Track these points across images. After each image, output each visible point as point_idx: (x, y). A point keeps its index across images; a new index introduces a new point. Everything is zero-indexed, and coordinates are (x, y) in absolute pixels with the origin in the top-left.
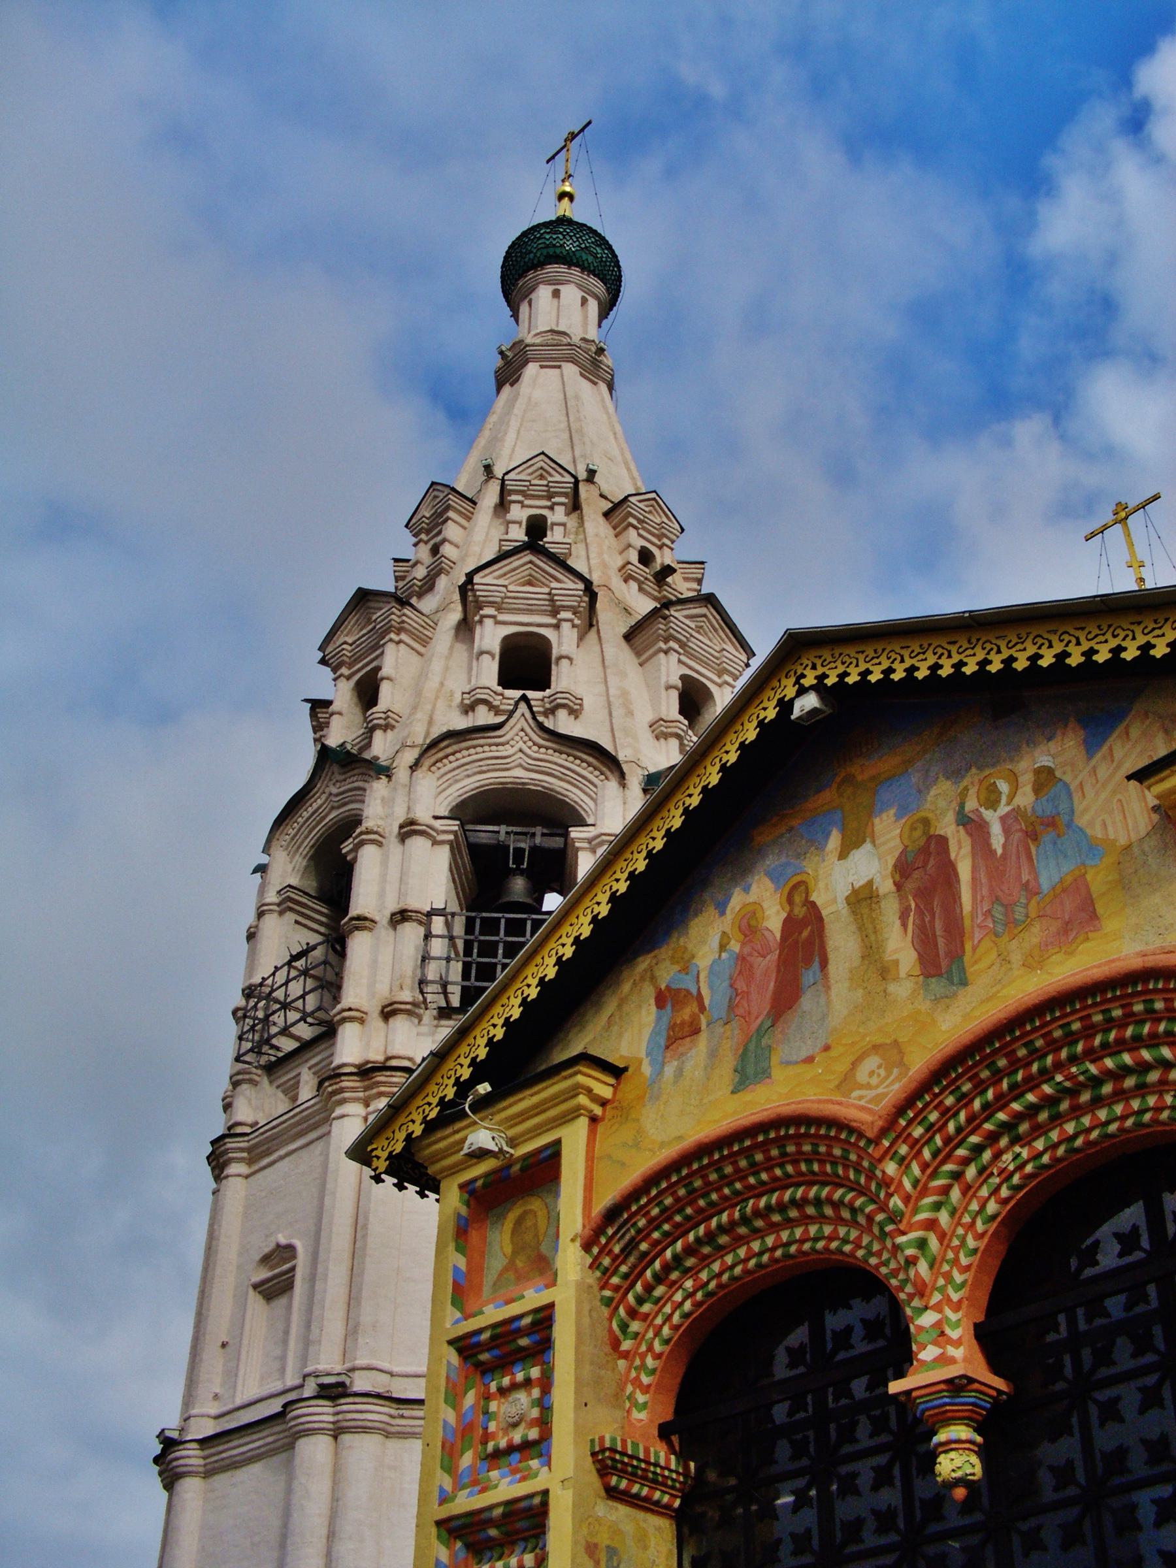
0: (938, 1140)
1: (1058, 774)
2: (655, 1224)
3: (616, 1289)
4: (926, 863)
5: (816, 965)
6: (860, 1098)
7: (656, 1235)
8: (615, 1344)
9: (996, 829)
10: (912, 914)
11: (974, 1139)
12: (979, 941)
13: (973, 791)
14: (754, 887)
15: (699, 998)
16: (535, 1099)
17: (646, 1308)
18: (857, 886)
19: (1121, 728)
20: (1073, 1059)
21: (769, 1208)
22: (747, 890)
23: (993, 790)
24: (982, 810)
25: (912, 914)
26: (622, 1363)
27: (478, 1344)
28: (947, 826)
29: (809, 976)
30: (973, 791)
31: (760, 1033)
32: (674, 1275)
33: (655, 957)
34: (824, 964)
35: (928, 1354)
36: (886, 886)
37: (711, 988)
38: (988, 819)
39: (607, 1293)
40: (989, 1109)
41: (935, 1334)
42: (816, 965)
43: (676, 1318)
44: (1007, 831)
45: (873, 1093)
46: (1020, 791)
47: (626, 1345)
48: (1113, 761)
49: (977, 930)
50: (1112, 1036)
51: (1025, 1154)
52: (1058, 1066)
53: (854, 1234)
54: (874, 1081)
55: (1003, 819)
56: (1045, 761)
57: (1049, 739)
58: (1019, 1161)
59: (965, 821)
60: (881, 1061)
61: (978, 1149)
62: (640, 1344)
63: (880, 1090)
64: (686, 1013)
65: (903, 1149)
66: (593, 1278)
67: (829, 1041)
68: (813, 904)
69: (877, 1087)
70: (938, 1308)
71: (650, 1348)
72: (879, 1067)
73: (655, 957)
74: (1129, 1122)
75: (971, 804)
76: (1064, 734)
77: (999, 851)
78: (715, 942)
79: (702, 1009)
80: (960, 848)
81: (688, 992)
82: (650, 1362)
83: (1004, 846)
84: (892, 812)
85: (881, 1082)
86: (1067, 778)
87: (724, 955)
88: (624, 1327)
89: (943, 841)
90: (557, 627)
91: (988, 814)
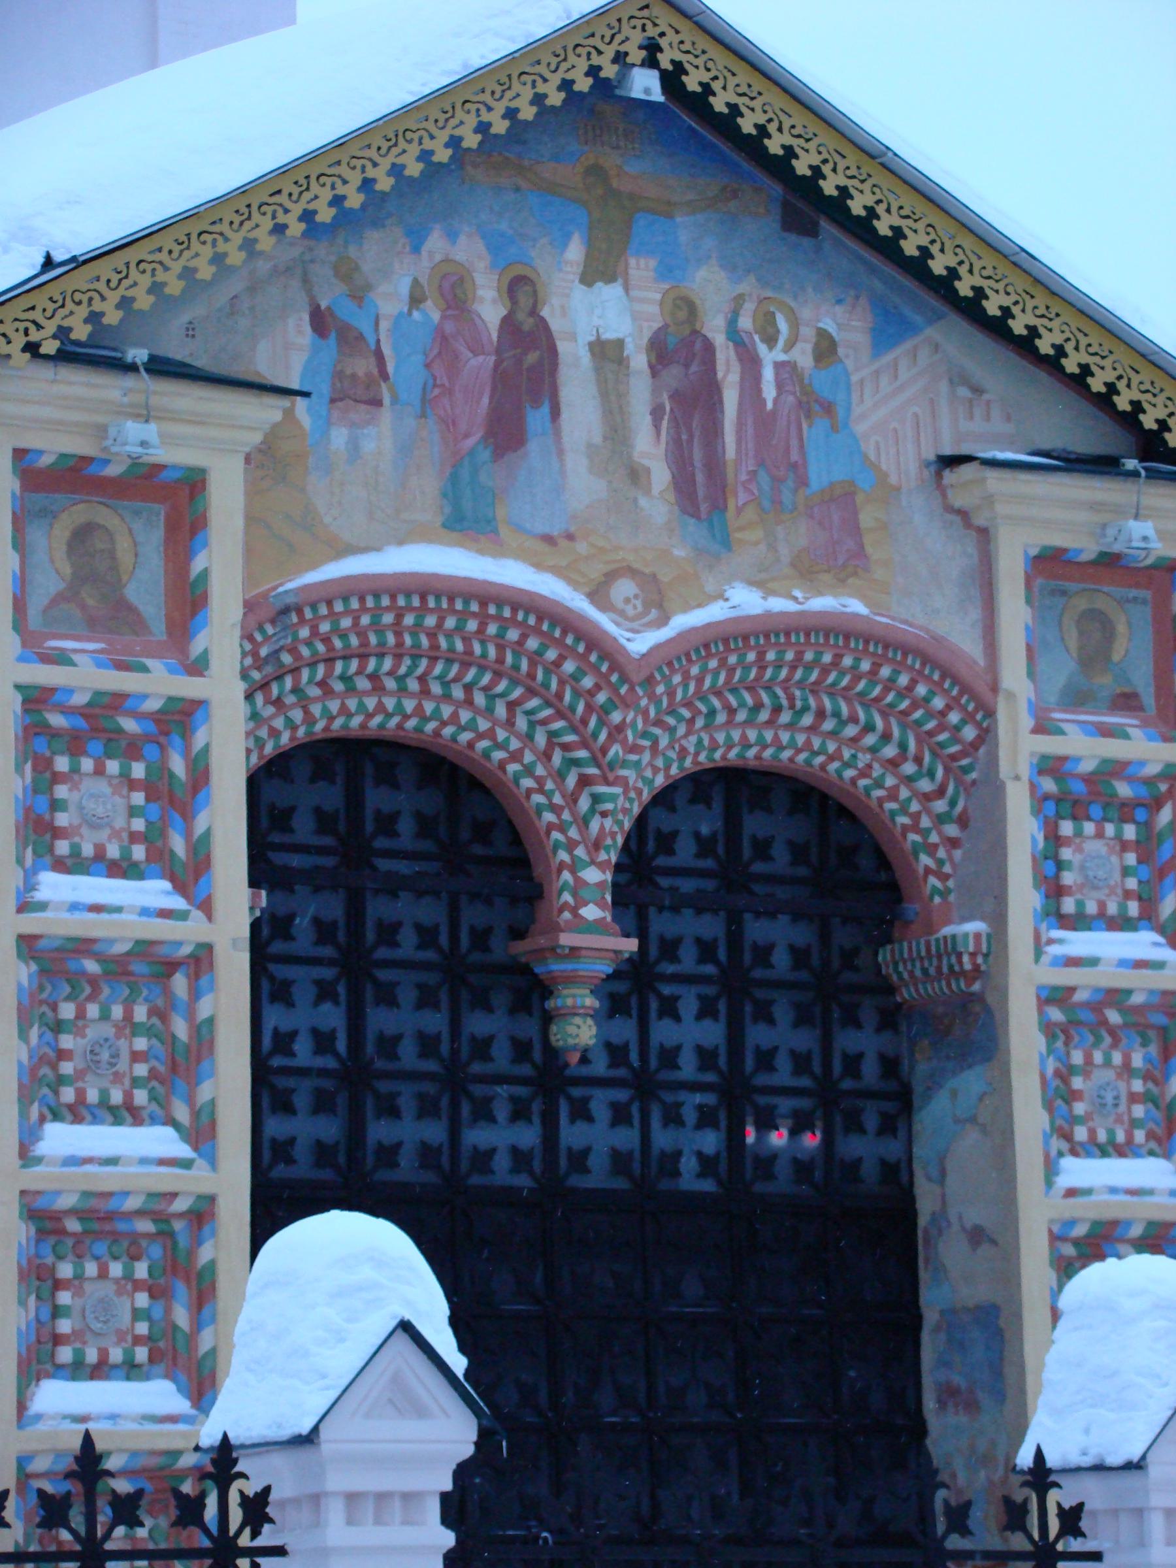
1: (841, 351)
4: (687, 366)
9: (768, 374)
10: (666, 417)
12: (744, 504)
13: (749, 307)
14: (463, 239)
19: (908, 345)
22: (452, 236)
23: (770, 318)
24: (756, 338)
25: (666, 417)
28: (715, 328)
29: (537, 419)
30: (749, 307)
33: (311, 249)
34: (555, 413)
36: (639, 361)
38: (762, 356)
41: (598, 896)
42: (546, 409)
44: (780, 386)
46: (799, 346)
48: (896, 377)
49: (740, 490)
53: (515, 744)
55: (778, 366)
56: (829, 325)
57: (839, 302)
64: (362, 366)
67: (573, 529)
68: (543, 320)
72: (636, 597)
73: (311, 249)
75: (745, 322)
76: (854, 306)
77: (770, 405)
78: (404, 287)
79: (384, 376)
80: (728, 371)
81: (361, 337)
83: (776, 401)
84: (653, 263)
86: (850, 364)
87: (416, 314)
89: (709, 348)
91: (762, 348)
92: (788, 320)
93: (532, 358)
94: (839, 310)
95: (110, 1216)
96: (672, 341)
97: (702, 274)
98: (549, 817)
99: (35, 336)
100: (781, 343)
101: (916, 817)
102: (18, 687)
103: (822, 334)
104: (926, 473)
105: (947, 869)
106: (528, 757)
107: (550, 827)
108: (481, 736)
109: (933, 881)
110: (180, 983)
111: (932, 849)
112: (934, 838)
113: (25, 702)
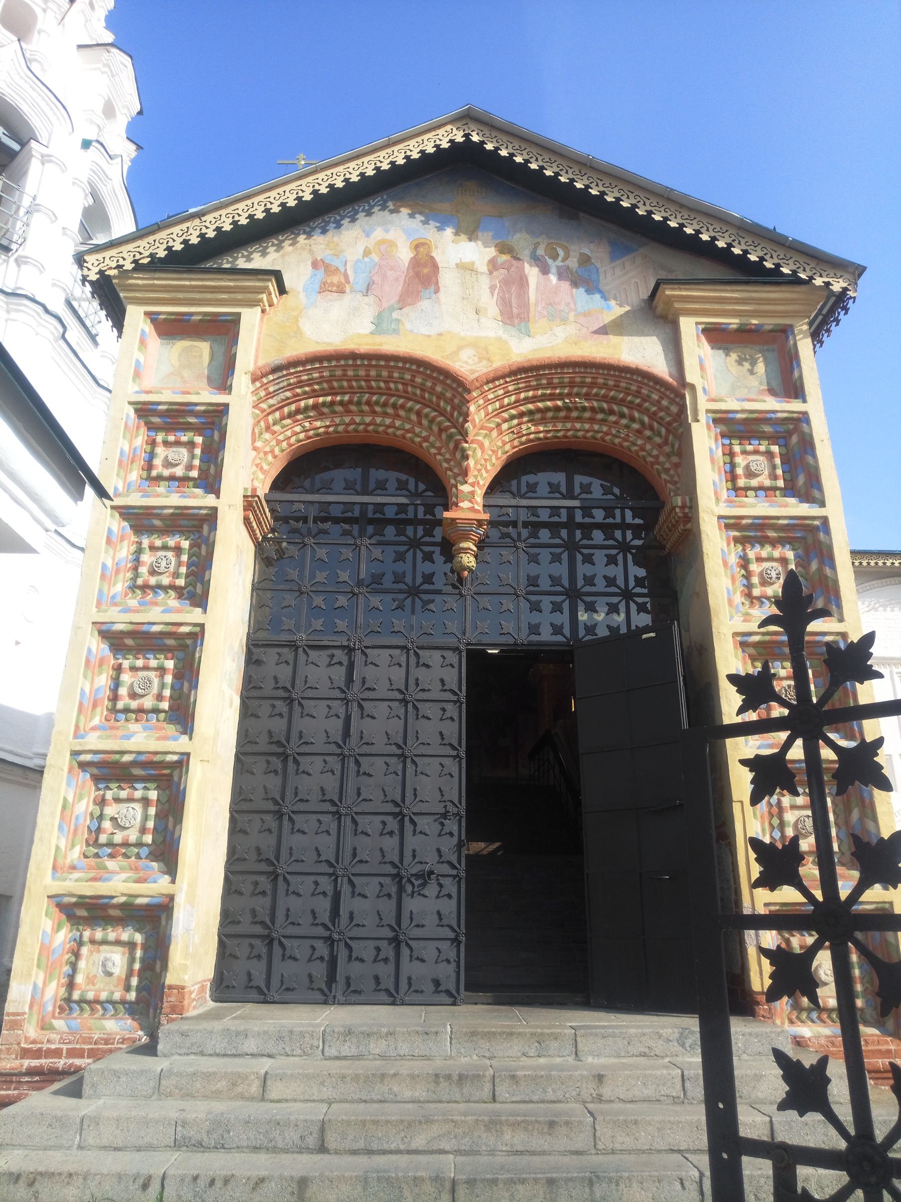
0: (497, 405)
1: (593, 261)
3: (263, 411)
5: (432, 288)
6: (462, 367)
7: (299, 391)
8: (254, 441)
11: (513, 412)
14: (392, 232)
15: (346, 275)
17: (277, 428)
20: (578, 395)
21: (377, 403)
22: (387, 231)
27: (155, 411)
31: (392, 309)
32: (300, 417)
34: (437, 291)
35: (465, 504)
36: (483, 268)
37: (355, 272)
40: (527, 400)
43: (293, 440)
45: (469, 367)
47: (259, 444)
50: (603, 392)
51: (533, 429)
52: (569, 395)
56: (586, 251)
58: (528, 431)
61: (512, 417)
63: (474, 367)
64: (335, 279)
65: (481, 402)
66: (251, 399)
68: (432, 258)
70: (473, 485)
71: (272, 451)
72: (475, 356)
74: (590, 434)
78: (361, 250)
79: (348, 282)
82: (270, 457)
84: (490, 234)
86: (598, 265)
87: (366, 259)
90: (44, 10)
92: (563, 250)
93: (426, 271)
94: (592, 246)
95: (148, 635)
97: (518, 235)
98: (445, 465)
99: (138, 256)
100: (560, 258)
101: (657, 457)
102: (130, 403)
103: (582, 254)
104: (643, 304)
105: (676, 479)
106: (432, 439)
107: (447, 469)
108: (408, 431)
109: (669, 485)
110: (206, 528)
111: (667, 471)
112: (667, 465)
113: (136, 411)
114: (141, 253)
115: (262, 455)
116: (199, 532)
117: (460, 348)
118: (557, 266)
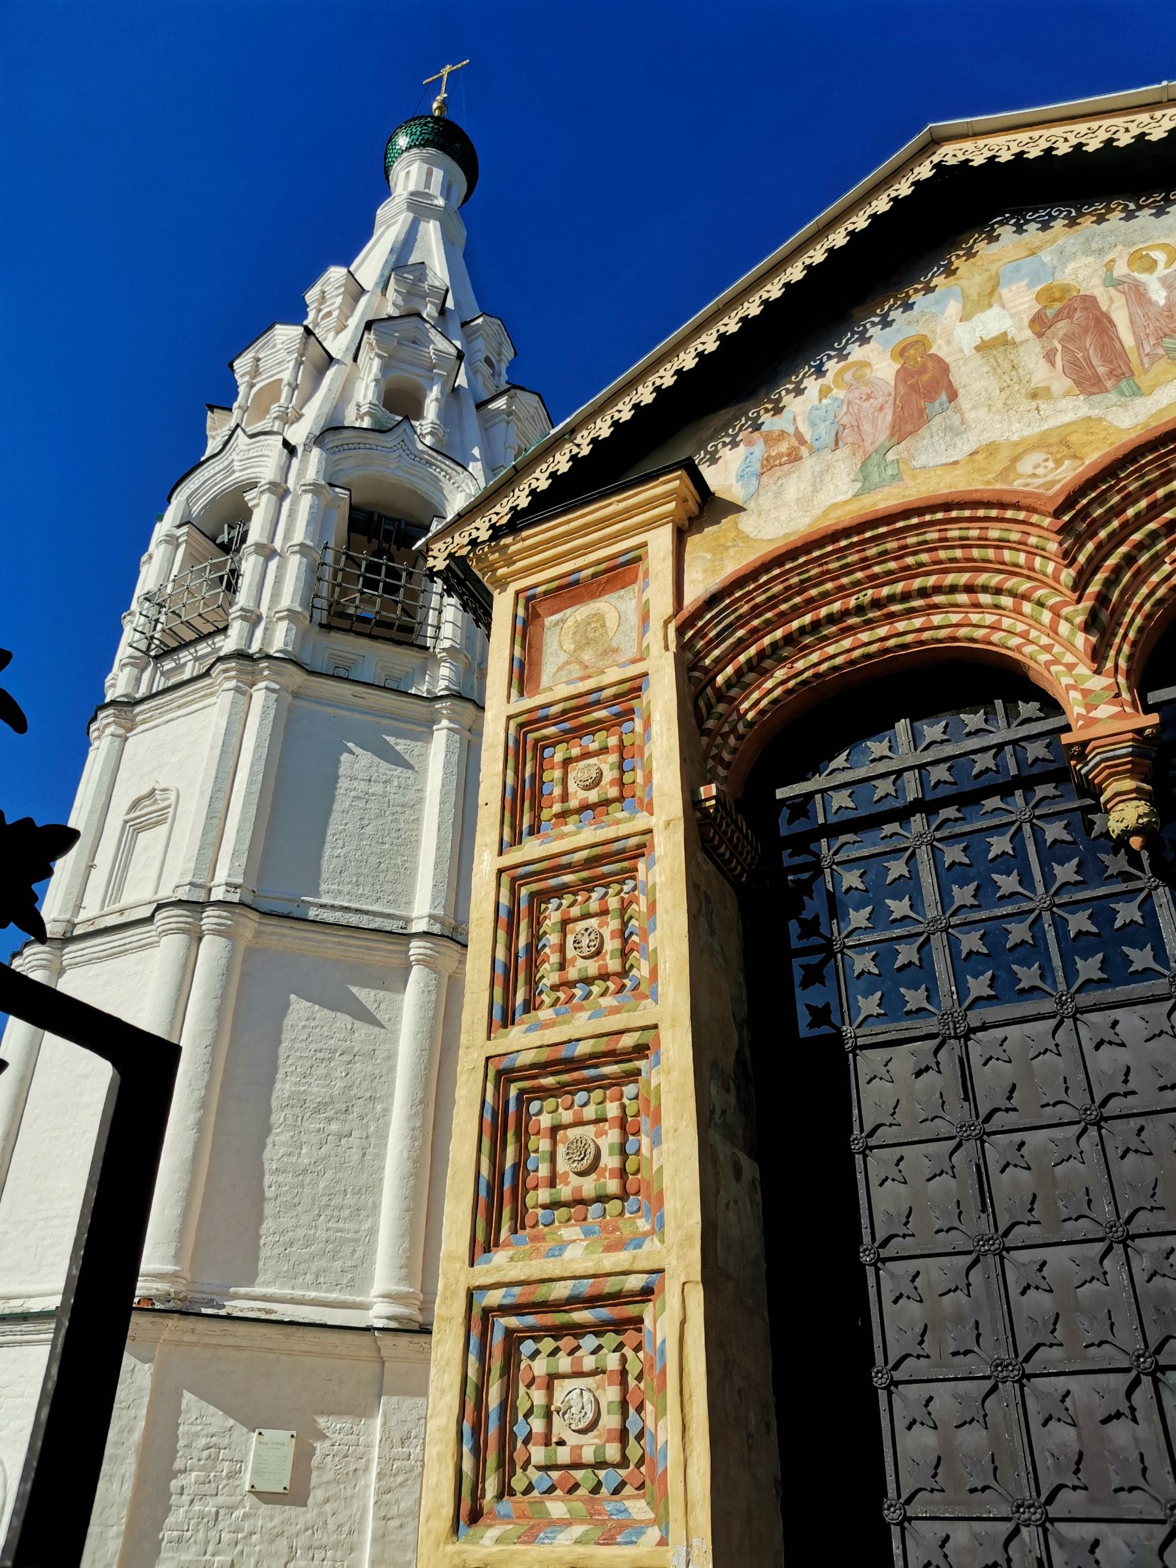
2: (756, 611)
6: (1028, 485)
8: (700, 722)
16: (622, 505)
18: (986, 338)
24: (1136, 274)
26: (705, 740)
32: (767, 663)
34: (953, 396)
37: (813, 425)
39: (697, 674)
47: (710, 724)
54: (1040, 471)
59: (1112, 282)
60: (1045, 456)
62: (723, 725)
63: (1049, 478)
64: (783, 447)
69: (1045, 475)
79: (802, 441)
85: (1052, 471)
88: (710, 707)
89: (1089, 302)
91: (1143, 277)
96: (1050, 313)
98: (1044, 657)
100: (1161, 265)
107: (1048, 664)
114: (497, 514)
115: (719, 740)
116: (634, 878)
117: (1016, 459)
118: (1159, 279)
